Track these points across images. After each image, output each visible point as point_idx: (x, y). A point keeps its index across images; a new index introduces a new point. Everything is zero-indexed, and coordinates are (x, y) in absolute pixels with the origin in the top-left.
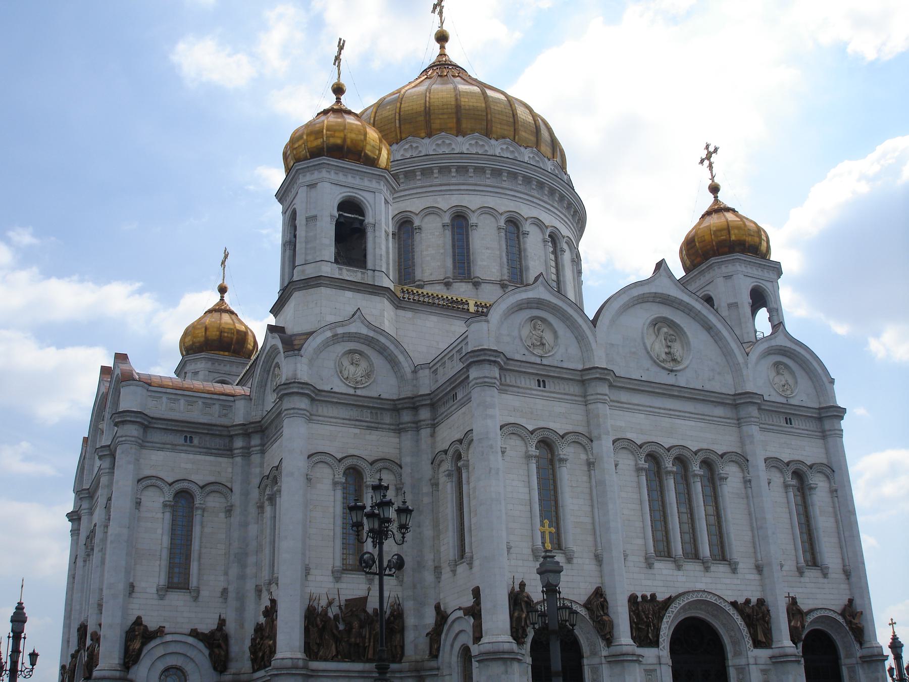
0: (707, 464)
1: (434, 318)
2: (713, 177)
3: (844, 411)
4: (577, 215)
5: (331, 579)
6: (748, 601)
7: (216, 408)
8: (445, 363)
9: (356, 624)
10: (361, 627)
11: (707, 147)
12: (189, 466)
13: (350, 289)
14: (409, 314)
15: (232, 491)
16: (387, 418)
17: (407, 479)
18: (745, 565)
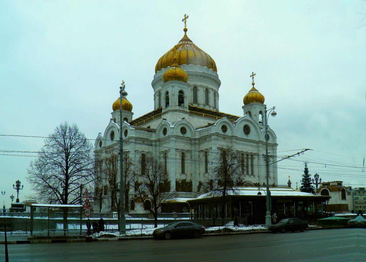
0: (252, 155)
1: (196, 118)
2: (253, 81)
3: (278, 144)
4: (218, 83)
5: (179, 175)
6: (256, 183)
7: (149, 135)
8: (203, 132)
9: (184, 185)
10: (185, 185)
11: (253, 73)
12: (144, 148)
13: (183, 113)
14: (192, 117)
15: (152, 153)
16: (189, 141)
17: (193, 155)
18: (256, 176)
